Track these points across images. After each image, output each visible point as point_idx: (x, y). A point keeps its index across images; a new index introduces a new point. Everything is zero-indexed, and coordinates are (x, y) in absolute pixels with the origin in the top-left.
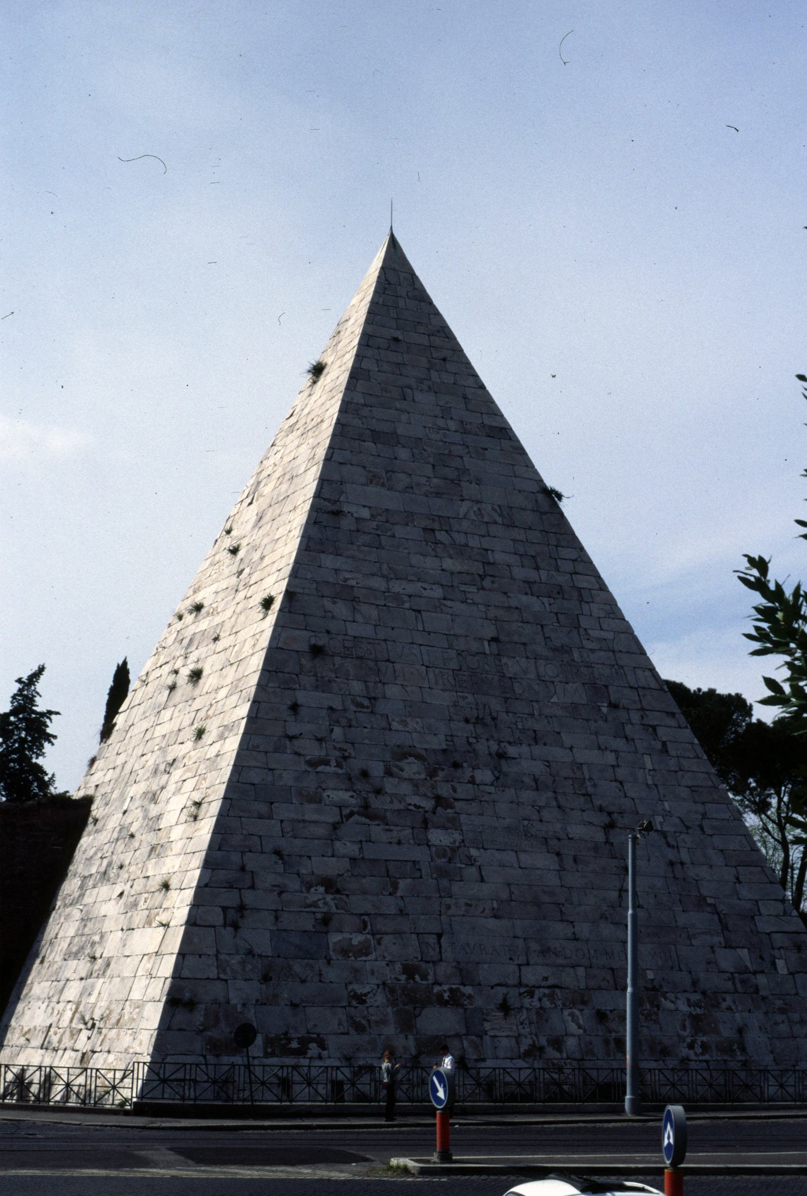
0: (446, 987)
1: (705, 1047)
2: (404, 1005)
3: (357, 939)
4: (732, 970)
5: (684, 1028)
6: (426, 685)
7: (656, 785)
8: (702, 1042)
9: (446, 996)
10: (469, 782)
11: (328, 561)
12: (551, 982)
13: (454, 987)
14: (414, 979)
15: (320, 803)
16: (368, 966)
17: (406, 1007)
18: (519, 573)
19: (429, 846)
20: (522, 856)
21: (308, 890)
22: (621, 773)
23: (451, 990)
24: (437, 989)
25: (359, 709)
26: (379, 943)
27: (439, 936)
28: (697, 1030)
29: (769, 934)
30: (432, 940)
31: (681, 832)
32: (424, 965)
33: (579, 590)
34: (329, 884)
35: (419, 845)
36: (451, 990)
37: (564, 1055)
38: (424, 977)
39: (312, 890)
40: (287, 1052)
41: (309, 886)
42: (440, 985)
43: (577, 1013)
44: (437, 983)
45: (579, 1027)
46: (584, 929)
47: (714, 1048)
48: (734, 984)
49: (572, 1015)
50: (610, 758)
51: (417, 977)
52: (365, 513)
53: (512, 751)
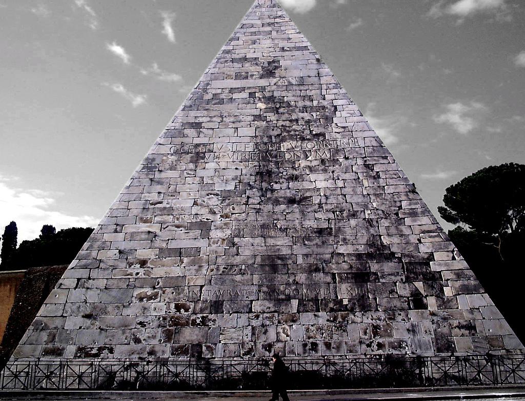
0: (199, 316)
1: (380, 346)
2: (170, 327)
3: (150, 292)
4: (409, 295)
5: (365, 333)
6: (231, 160)
7: (369, 195)
8: (378, 343)
9: (198, 321)
10: (244, 204)
11: (193, 113)
12: (273, 310)
13: (205, 315)
14: (179, 311)
15: (151, 222)
16: (153, 306)
17: (170, 328)
18: (301, 104)
19: (208, 238)
20: (269, 240)
21: (130, 266)
22: (344, 191)
23: (203, 317)
24: (193, 317)
25: (188, 176)
26: (164, 293)
27: (202, 287)
28: (376, 334)
29: (440, 272)
30: (198, 289)
31: (382, 218)
32: (188, 303)
33: (335, 107)
34: (143, 263)
35: (203, 239)
36: (203, 317)
37: (272, 354)
38: (187, 310)
39: (133, 266)
40: (88, 355)
41: (130, 265)
42: (196, 314)
43: (287, 327)
44: (194, 313)
45: (288, 336)
46: (302, 278)
47: (387, 346)
48: (409, 304)
49: (284, 329)
50: (340, 184)
51: (182, 310)
52: (219, 91)
53: (276, 186)
